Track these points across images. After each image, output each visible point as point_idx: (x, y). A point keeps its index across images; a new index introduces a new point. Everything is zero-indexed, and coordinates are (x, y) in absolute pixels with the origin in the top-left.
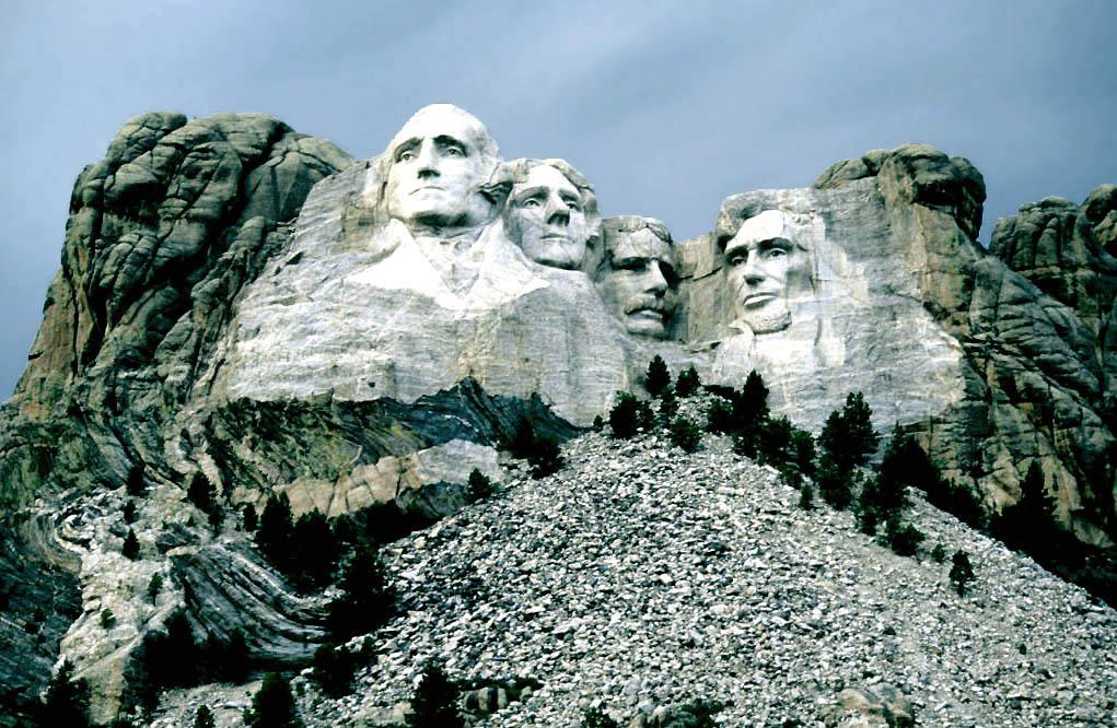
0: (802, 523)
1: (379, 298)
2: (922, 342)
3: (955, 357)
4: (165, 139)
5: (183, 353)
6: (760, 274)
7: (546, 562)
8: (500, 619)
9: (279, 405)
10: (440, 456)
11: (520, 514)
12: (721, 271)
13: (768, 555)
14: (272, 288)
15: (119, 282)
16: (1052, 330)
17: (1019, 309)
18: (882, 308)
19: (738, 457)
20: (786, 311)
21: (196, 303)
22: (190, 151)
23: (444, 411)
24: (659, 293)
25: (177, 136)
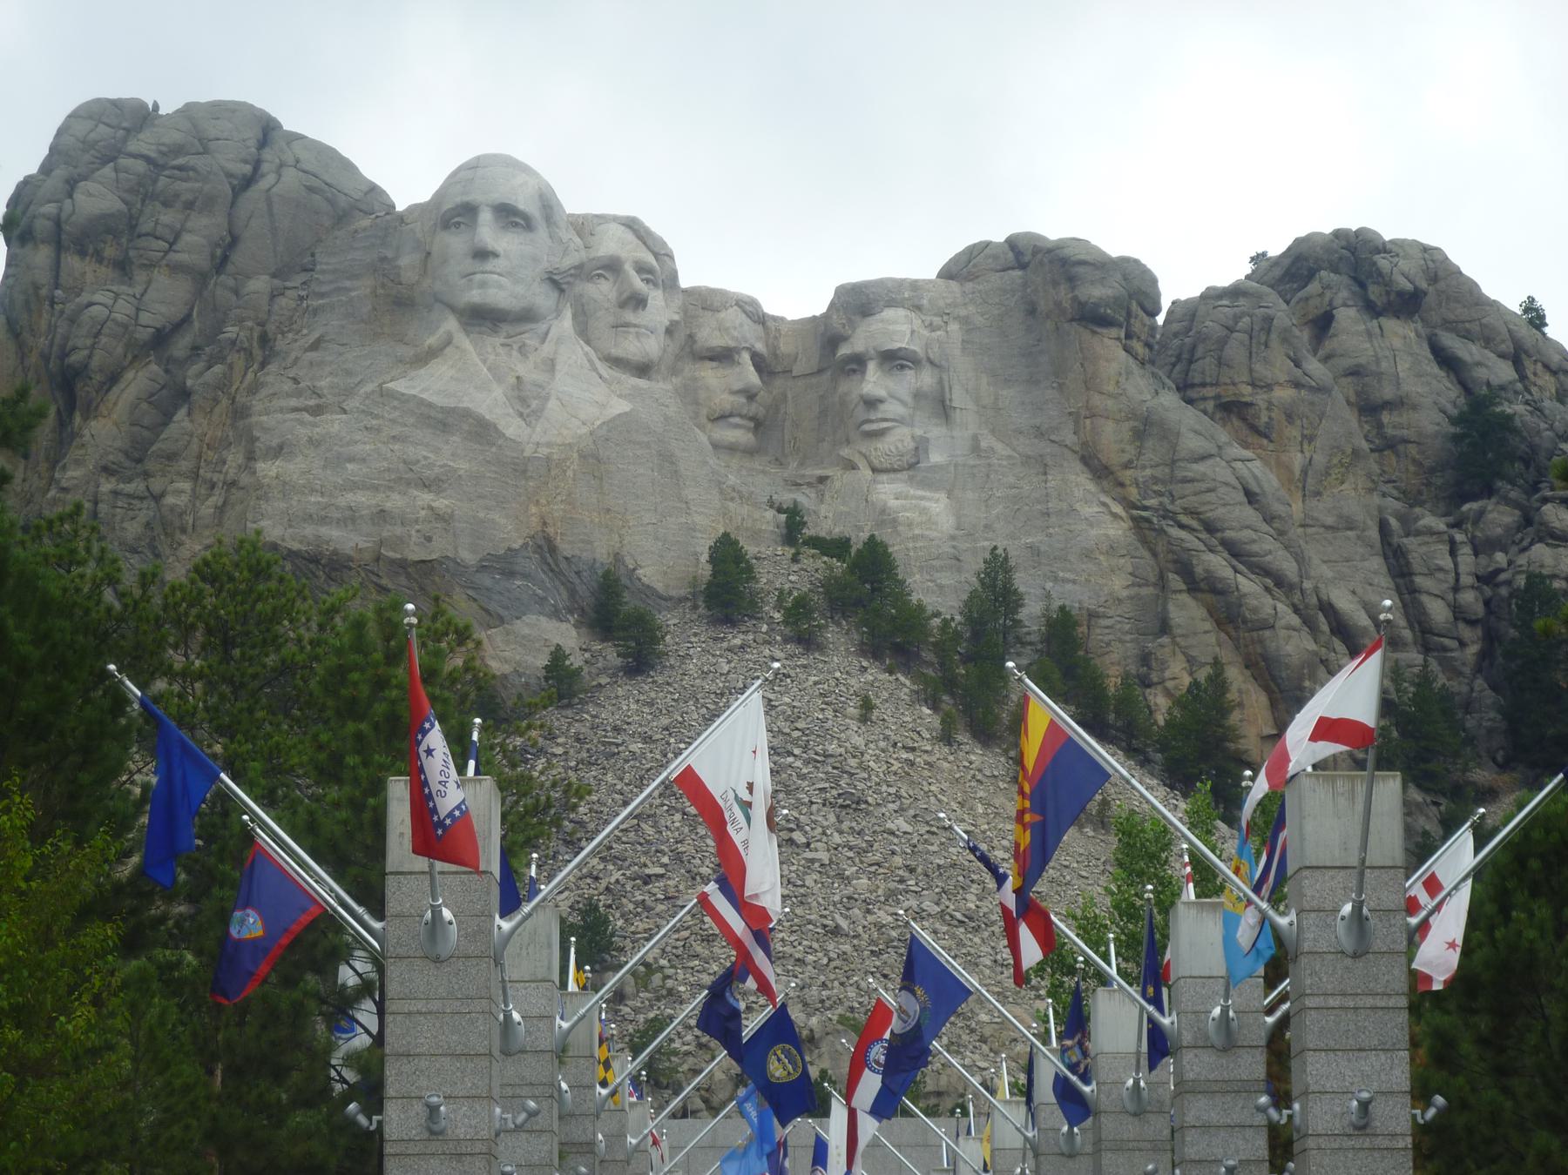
0: (946, 765)
1: (429, 417)
2: (1077, 506)
3: (1118, 531)
4: (133, 146)
5: (185, 465)
6: (882, 393)
7: (658, 801)
8: (613, 880)
9: (314, 559)
10: (512, 637)
11: (616, 729)
12: (827, 375)
13: (912, 812)
14: (288, 386)
15: (95, 363)
16: (1242, 497)
17: (1200, 468)
18: (1029, 457)
19: (865, 664)
20: (912, 445)
21: (195, 397)
22: (164, 167)
23: (511, 574)
24: (750, 396)
25: (143, 143)
